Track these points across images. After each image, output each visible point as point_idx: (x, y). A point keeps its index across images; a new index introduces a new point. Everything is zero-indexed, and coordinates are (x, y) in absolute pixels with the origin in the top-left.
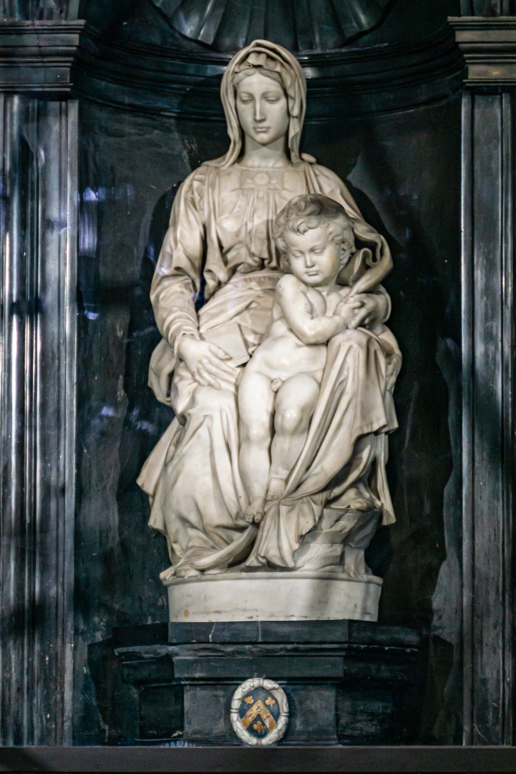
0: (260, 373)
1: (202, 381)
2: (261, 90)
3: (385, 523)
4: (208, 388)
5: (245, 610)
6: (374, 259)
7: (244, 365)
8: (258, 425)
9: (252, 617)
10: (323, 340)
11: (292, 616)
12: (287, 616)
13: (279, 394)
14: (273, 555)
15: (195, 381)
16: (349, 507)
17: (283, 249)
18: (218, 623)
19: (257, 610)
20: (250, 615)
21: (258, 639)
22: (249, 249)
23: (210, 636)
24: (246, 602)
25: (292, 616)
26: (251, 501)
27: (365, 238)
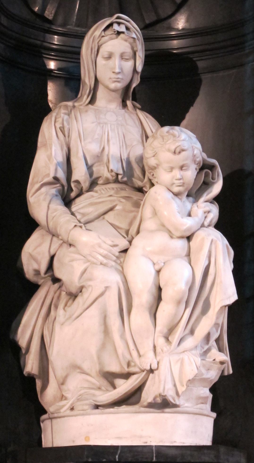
0: (144, 255)
1: (95, 261)
2: (113, 52)
3: (226, 374)
4: (101, 266)
5: (141, 437)
6: (213, 178)
7: (125, 251)
8: (143, 296)
9: (146, 443)
10: (188, 234)
11: (175, 442)
12: (172, 442)
13: (161, 274)
14: (170, 395)
15: (89, 261)
16: (214, 360)
17: (156, 166)
18: (122, 447)
19: (150, 437)
20: (145, 441)
21: (153, 459)
22: (108, 168)
23: (117, 457)
24: (142, 430)
25: (175, 442)
26: (141, 353)
27: (210, 162)
